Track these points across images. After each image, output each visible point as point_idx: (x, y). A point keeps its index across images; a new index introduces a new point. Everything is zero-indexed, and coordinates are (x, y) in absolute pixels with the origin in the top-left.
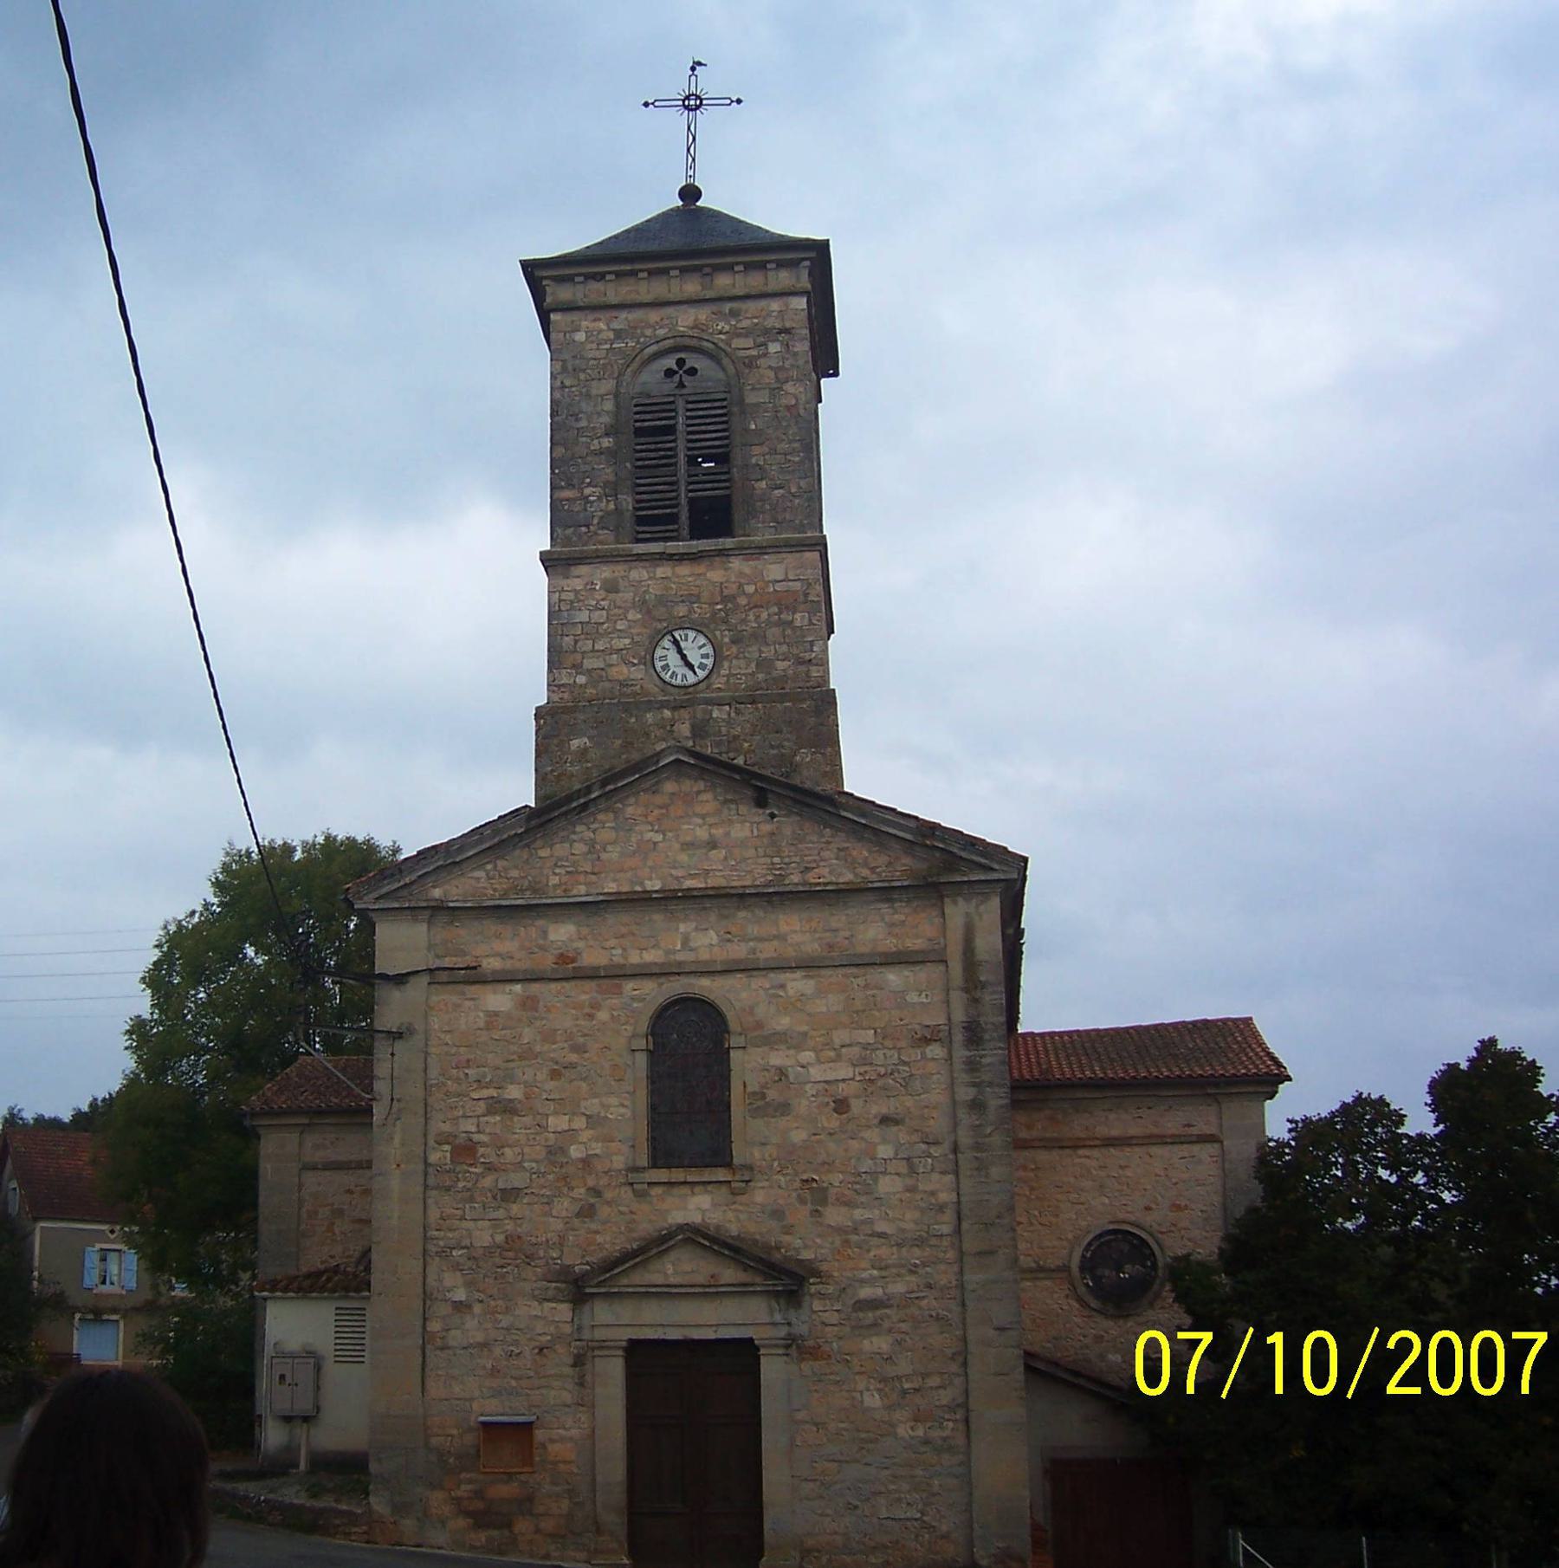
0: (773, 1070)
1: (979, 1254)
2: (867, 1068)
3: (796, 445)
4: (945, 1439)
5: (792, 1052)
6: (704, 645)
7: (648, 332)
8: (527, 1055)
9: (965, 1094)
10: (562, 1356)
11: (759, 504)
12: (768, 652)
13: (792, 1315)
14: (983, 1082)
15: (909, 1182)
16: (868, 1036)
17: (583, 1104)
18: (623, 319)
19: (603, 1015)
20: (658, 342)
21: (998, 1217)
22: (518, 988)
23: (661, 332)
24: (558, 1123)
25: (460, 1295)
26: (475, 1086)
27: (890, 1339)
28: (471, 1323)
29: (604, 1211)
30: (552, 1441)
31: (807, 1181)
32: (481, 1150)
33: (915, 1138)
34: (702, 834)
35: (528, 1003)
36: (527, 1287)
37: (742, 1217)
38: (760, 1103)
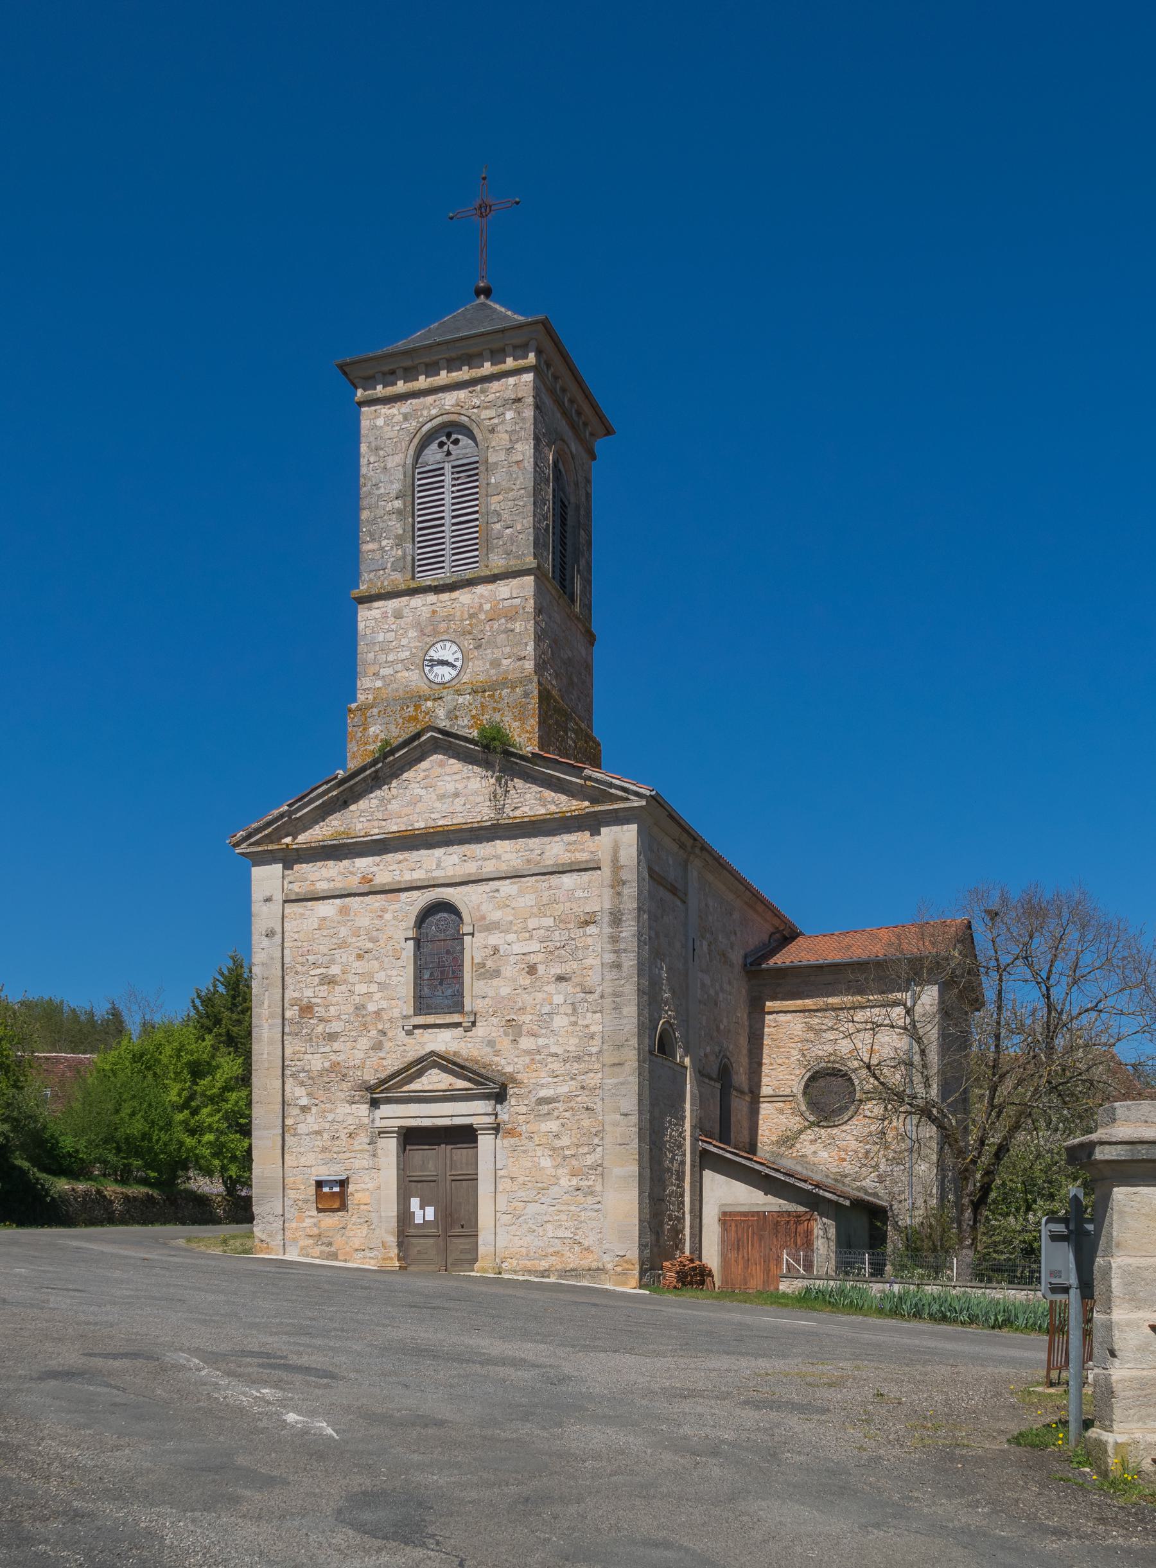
0: (490, 947)
1: (614, 1065)
2: (549, 943)
3: (522, 492)
4: (589, 1187)
5: (503, 934)
6: (456, 652)
7: (425, 413)
8: (343, 945)
9: (609, 958)
10: (363, 1139)
11: (495, 541)
12: (498, 654)
13: (498, 1106)
14: (619, 950)
15: (573, 1019)
16: (549, 922)
17: (376, 975)
18: (407, 406)
19: (388, 916)
20: (431, 420)
21: (626, 1041)
22: (338, 901)
23: (434, 412)
24: (362, 988)
25: (304, 1101)
26: (312, 966)
27: (558, 1122)
28: (310, 1119)
29: (388, 1045)
30: (357, 1191)
31: (509, 1021)
32: (316, 1009)
33: (578, 989)
34: (451, 788)
35: (344, 911)
36: (342, 1095)
37: (469, 1045)
38: (482, 970)
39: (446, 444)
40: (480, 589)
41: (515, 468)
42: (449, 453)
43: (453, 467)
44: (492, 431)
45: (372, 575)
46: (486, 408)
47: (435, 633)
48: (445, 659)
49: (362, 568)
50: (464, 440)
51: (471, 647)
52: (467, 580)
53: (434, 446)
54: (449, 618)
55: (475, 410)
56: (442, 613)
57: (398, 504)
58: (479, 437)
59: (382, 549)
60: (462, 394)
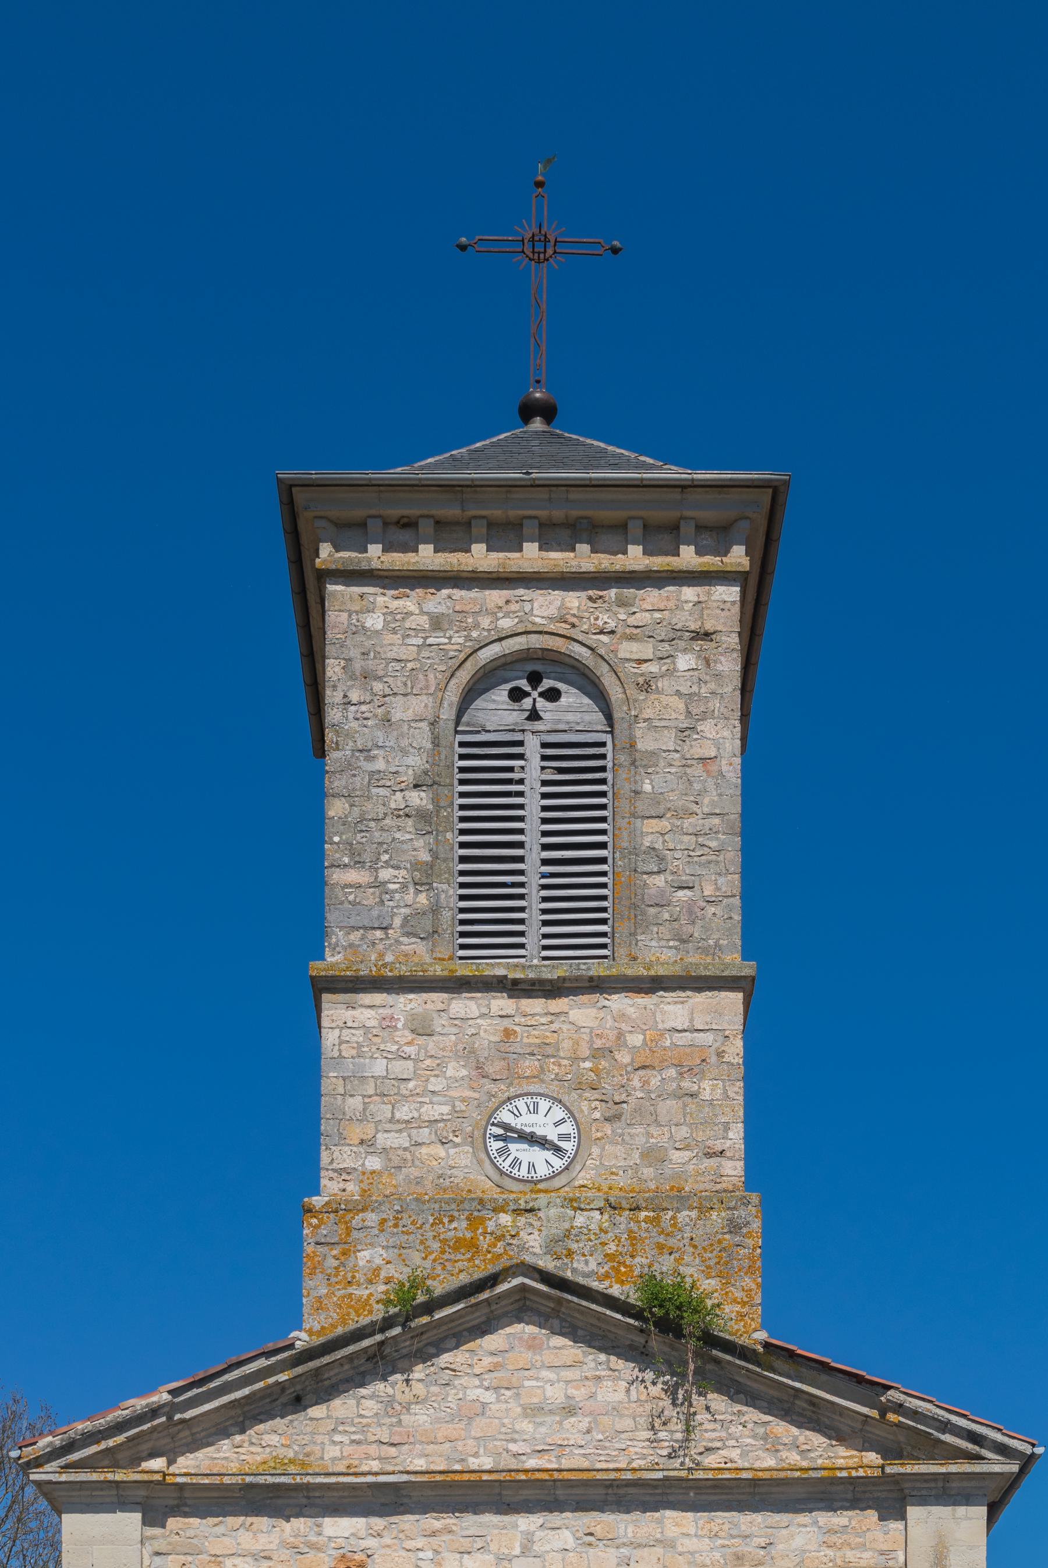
3: (716, 821)
6: (562, 1121)
18: (440, 601)
20: (500, 639)
23: (506, 624)
39: (528, 694)
40: (618, 1002)
41: (697, 770)
42: (534, 715)
43: (544, 745)
44: (646, 687)
45: (355, 936)
46: (631, 638)
47: (512, 1076)
48: (540, 1132)
49: (332, 917)
50: (571, 697)
51: (597, 1115)
52: (591, 979)
53: (500, 695)
54: (544, 1051)
55: (604, 638)
56: (527, 1038)
57: (418, 799)
58: (615, 693)
59: (380, 885)
60: (574, 600)
